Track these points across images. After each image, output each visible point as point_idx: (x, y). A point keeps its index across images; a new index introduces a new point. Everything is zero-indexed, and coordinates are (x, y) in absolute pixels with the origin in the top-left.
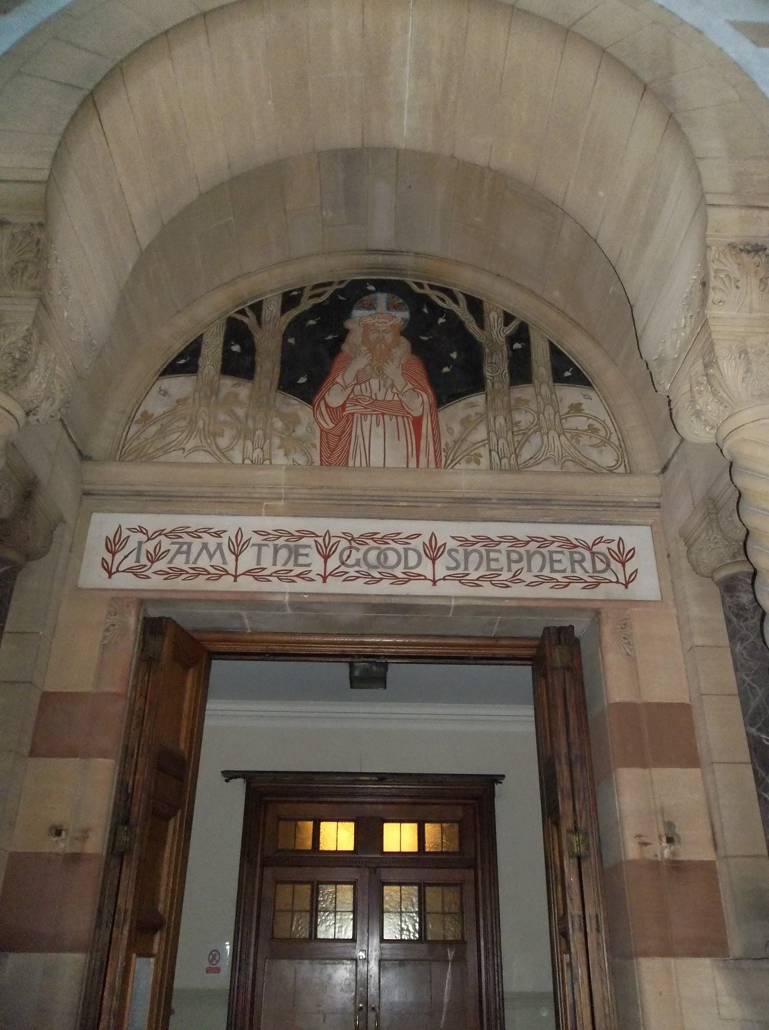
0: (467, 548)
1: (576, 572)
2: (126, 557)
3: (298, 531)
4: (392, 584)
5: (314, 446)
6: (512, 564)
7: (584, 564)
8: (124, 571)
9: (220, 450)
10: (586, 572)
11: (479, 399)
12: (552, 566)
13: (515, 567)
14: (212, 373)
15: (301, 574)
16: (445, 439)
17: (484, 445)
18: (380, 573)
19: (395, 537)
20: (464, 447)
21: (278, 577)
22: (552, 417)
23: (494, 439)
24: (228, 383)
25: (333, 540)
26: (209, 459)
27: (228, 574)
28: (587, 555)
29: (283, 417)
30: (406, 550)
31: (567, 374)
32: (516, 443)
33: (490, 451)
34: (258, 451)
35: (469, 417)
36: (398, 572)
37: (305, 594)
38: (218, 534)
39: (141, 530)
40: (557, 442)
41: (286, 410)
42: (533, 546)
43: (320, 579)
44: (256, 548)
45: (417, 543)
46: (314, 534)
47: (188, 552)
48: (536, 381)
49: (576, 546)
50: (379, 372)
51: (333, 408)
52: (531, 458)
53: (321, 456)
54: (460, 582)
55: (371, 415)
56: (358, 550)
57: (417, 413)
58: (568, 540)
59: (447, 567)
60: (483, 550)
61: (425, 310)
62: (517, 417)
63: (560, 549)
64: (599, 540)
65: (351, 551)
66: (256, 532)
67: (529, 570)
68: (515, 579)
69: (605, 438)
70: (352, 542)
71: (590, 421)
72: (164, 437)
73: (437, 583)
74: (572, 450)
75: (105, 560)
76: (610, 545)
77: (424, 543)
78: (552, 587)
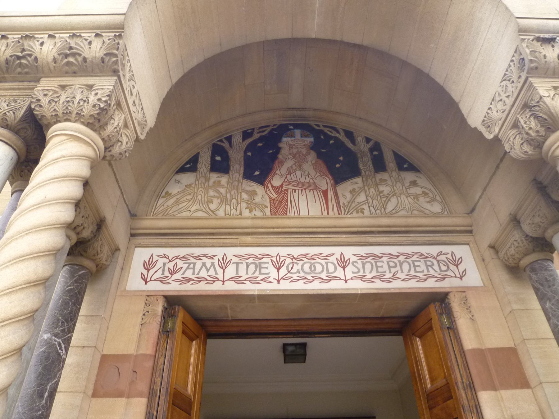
0: (363, 260)
1: (429, 272)
2: (156, 272)
3: (260, 254)
4: (320, 283)
5: (267, 207)
6: (392, 269)
8: (155, 280)
9: (211, 211)
10: (436, 272)
11: (359, 180)
12: (415, 269)
13: (393, 270)
14: (205, 171)
15: (264, 279)
16: (342, 201)
17: (365, 204)
18: (312, 277)
19: (319, 256)
20: (353, 205)
21: (250, 281)
22: (401, 188)
23: (371, 201)
24: (214, 177)
25: (282, 259)
26: (204, 215)
27: (218, 280)
28: (435, 262)
29: (247, 192)
30: (327, 263)
31: (405, 166)
32: (383, 202)
33: (369, 207)
34: (234, 211)
35: (354, 189)
36: (323, 276)
38: (212, 258)
39: (165, 256)
40: (406, 201)
41: (249, 188)
42: (402, 258)
43: (276, 282)
44: (235, 265)
45: (333, 259)
46: (270, 255)
47: (194, 268)
48: (389, 171)
49: (427, 257)
50: (300, 168)
51: (276, 187)
52: (393, 210)
55: (298, 190)
56: (297, 264)
57: (324, 188)
58: (422, 254)
59: (352, 272)
61: (322, 137)
62: (381, 188)
63: (418, 259)
64: (440, 253)
65: (293, 265)
66: (234, 255)
67: (402, 272)
68: (394, 277)
69: (433, 198)
70: (293, 259)
71: (423, 190)
72: (179, 205)
73: (348, 282)
74: (416, 205)
75: (143, 274)
76: (448, 256)
77: (337, 259)
78: (417, 281)
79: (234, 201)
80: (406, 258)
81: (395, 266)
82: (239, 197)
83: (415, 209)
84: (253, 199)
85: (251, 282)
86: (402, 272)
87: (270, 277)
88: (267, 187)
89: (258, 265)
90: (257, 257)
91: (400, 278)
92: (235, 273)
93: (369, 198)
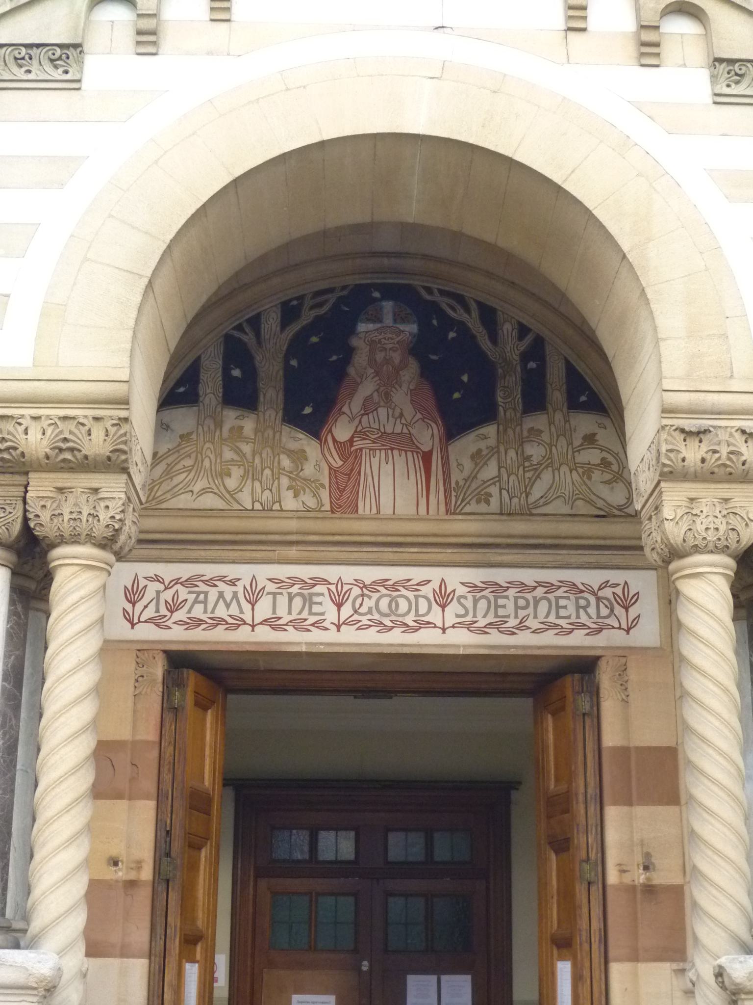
0: (476, 594)
1: (580, 618)
2: (146, 607)
3: (310, 579)
4: (403, 632)
5: (323, 486)
6: (520, 611)
7: (589, 610)
8: (145, 622)
9: (228, 492)
10: (590, 618)
11: (490, 430)
12: (557, 613)
13: (522, 613)
14: (214, 402)
15: (316, 623)
17: (494, 483)
18: (391, 621)
19: (405, 583)
20: (474, 486)
21: (293, 626)
22: (565, 450)
23: (505, 477)
24: (231, 416)
25: (346, 588)
26: (219, 504)
27: (245, 623)
28: (592, 599)
29: (291, 453)
30: (416, 597)
31: (583, 398)
33: (501, 490)
34: (267, 492)
35: (479, 451)
36: (409, 620)
37: (321, 644)
38: (233, 583)
39: (157, 579)
40: (568, 478)
41: (293, 445)
42: (540, 592)
43: (334, 628)
44: (271, 597)
46: (326, 581)
47: (205, 602)
48: (550, 410)
49: (582, 591)
50: (387, 399)
51: (341, 443)
52: (542, 497)
53: (330, 497)
54: (468, 630)
55: (380, 450)
56: (370, 597)
57: (426, 448)
58: (574, 585)
60: (491, 596)
63: (566, 595)
64: (605, 585)
65: (363, 599)
66: (269, 580)
67: (535, 617)
68: (521, 626)
69: (618, 473)
71: (604, 454)
72: (171, 478)
73: (447, 631)
74: (584, 487)
75: (126, 611)
76: (614, 590)
77: (434, 590)
78: (556, 634)
79: (267, 472)
80: (546, 593)
81: (526, 607)
82: (276, 464)
83: (581, 496)
84: (300, 469)
85: (296, 629)
86: (535, 617)
87: (325, 619)
88: (325, 443)
89: (307, 597)
90: (306, 583)
91: (531, 628)
92: (272, 612)
93: (503, 470)
